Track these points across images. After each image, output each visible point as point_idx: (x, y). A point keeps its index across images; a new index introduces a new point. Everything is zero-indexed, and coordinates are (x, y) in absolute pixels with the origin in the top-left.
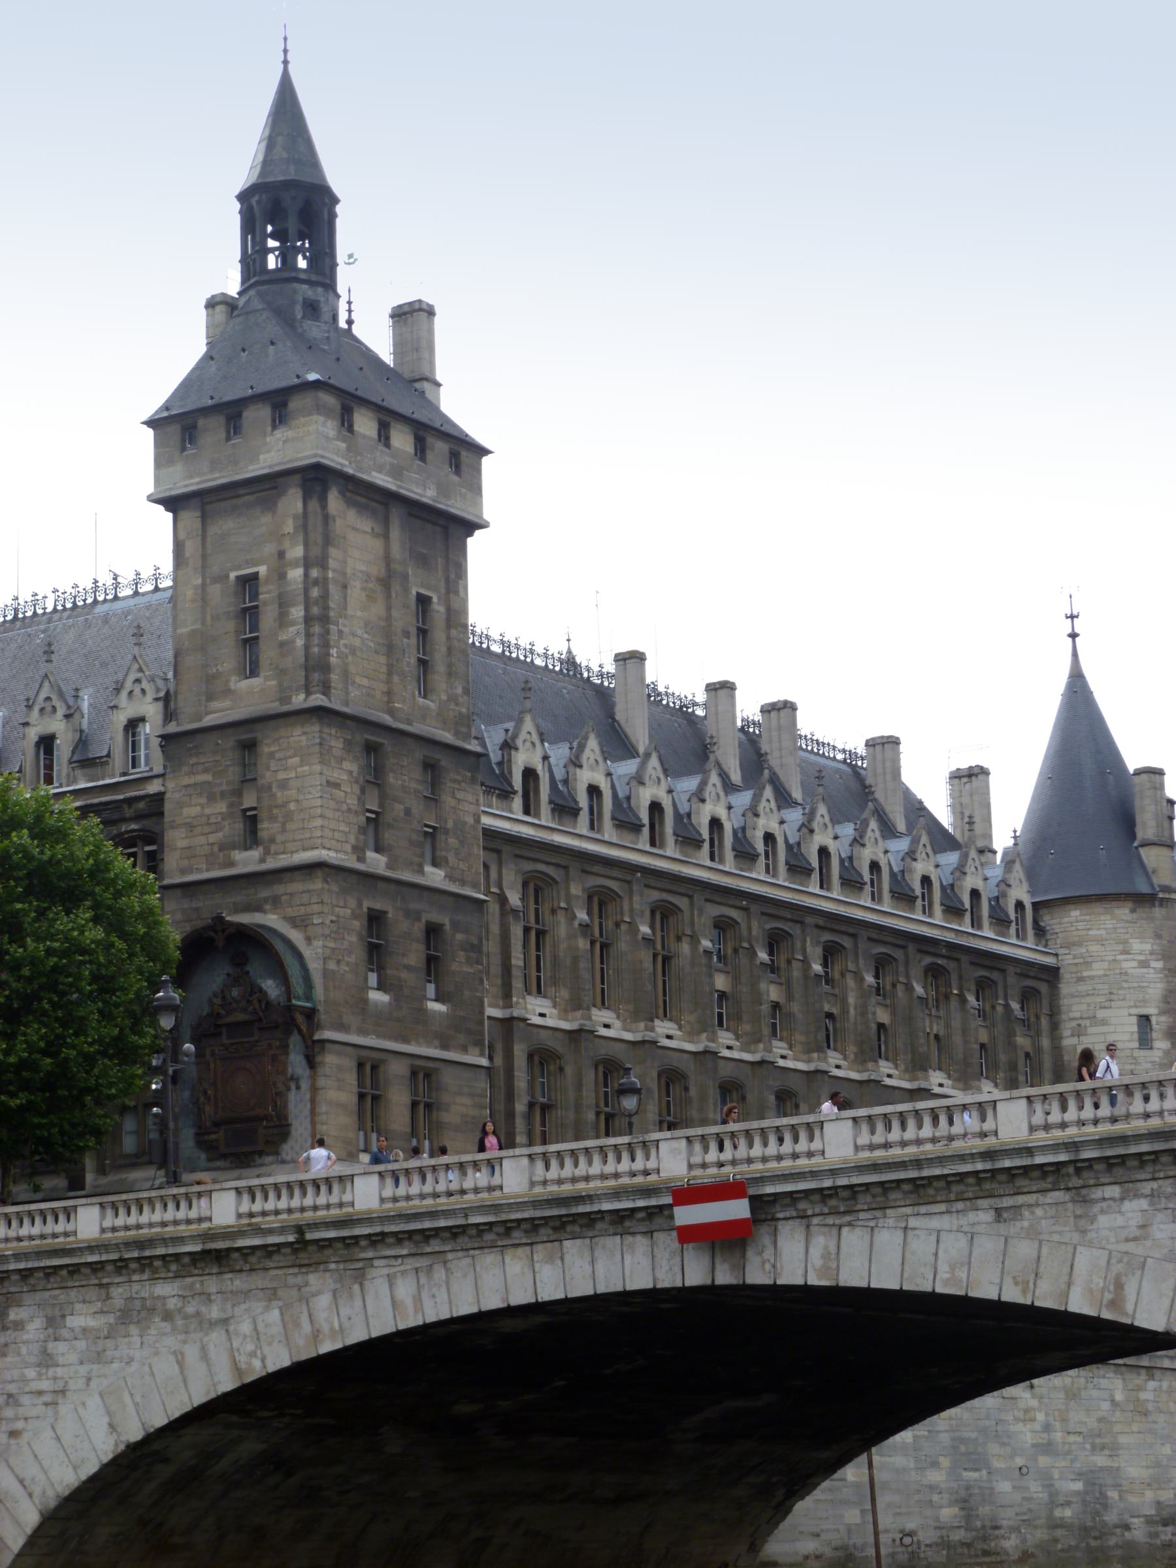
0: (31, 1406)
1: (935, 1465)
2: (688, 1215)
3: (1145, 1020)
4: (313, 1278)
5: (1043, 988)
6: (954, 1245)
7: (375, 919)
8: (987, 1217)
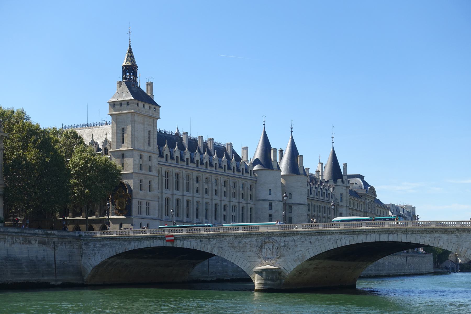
0: (91, 255)
1: (219, 262)
2: (167, 239)
3: (270, 190)
4: (125, 242)
5: (254, 184)
6: (196, 244)
7: (141, 181)
8: (199, 241)
